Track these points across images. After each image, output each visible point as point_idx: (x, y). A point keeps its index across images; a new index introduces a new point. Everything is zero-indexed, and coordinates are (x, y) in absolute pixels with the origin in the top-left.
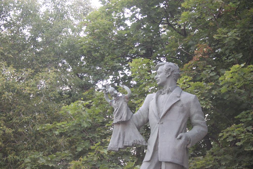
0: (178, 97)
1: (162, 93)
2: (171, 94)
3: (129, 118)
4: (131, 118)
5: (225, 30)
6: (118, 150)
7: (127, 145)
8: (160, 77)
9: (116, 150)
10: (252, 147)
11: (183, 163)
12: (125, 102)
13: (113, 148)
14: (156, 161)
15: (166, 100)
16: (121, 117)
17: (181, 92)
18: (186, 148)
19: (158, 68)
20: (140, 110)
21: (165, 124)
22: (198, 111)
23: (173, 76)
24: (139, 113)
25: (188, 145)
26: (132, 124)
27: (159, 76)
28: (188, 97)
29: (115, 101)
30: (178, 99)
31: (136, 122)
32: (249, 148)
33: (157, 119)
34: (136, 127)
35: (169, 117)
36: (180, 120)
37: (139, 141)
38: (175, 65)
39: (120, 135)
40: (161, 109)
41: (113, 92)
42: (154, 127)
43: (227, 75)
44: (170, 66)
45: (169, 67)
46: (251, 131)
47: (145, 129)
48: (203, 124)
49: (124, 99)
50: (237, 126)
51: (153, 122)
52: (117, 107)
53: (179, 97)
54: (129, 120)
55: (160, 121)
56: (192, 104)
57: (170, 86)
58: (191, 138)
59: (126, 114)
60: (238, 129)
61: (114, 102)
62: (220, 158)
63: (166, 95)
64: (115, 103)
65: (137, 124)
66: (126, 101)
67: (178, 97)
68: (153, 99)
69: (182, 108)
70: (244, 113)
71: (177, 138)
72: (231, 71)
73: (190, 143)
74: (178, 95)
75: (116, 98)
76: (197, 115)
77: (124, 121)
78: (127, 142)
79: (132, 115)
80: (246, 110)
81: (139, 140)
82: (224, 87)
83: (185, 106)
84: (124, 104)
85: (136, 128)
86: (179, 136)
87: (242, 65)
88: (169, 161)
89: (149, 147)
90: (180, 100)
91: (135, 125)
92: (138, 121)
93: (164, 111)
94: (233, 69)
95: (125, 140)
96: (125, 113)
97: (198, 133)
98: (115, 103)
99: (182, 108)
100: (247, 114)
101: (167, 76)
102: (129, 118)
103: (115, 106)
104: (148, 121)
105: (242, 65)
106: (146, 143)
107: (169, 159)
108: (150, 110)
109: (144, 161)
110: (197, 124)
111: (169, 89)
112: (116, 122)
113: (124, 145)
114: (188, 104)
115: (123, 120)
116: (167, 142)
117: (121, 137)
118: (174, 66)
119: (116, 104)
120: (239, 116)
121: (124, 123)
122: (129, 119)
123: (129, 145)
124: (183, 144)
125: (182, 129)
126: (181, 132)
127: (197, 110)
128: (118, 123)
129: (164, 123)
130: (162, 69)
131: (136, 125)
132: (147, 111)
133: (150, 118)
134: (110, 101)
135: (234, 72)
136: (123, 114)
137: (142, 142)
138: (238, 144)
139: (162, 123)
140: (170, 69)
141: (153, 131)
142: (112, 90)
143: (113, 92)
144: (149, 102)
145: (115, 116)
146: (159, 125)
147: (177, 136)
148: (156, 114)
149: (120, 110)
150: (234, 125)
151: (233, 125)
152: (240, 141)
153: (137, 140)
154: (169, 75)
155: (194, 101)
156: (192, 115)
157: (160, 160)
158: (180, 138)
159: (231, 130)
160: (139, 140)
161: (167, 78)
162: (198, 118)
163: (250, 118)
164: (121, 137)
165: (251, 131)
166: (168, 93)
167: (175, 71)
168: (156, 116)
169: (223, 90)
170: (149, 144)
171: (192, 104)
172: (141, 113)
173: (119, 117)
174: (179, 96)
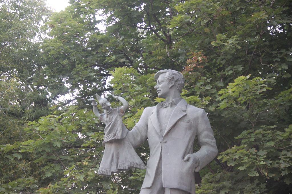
0: (183, 111)
1: (164, 107)
2: (176, 107)
3: (124, 135)
4: (127, 136)
5: (224, 36)
6: (110, 174)
7: (122, 168)
8: (162, 87)
9: (108, 174)
10: (257, 172)
11: (191, 190)
12: (120, 116)
13: (105, 172)
14: (158, 186)
15: (169, 114)
16: (115, 134)
17: (187, 105)
18: (194, 171)
19: (158, 77)
20: (137, 127)
21: (169, 143)
22: (207, 128)
23: (177, 86)
24: (136, 130)
25: (196, 168)
26: (127, 142)
27: (160, 86)
28: (196, 112)
29: (107, 115)
30: (184, 114)
31: (132, 140)
32: (254, 174)
33: (159, 137)
34: (132, 147)
35: (173, 135)
36: (187, 139)
37: (137, 164)
38: (179, 73)
39: (113, 156)
40: (164, 125)
41: (105, 104)
42: (155, 147)
43: (231, 89)
44: (173, 74)
45: (173, 76)
46: (255, 153)
47: (143, 148)
48: (212, 143)
49: (119, 112)
50: (238, 147)
51: (154, 140)
52: (110, 122)
53: (185, 111)
54: (125, 138)
55: (163, 140)
56: (200, 119)
57: (173, 98)
58: (200, 160)
59: (121, 131)
60: (241, 151)
61: (106, 115)
62: (218, 185)
63: (169, 108)
64: (106, 118)
65: (133, 143)
66: (121, 115)
67: (183, 111)
68: (152, 113)
69: (189, 124)
70: (245, 132)
71: (184, 160)
72: (235, 84)
73: (198, 166)
74: (184, 109)
75: (108, 112)
76: (205, 133)
77: (118, 139)
78: (123, 165)
79: (128, 132)
80: (246, 129)
81: (136, 163)
82: (223, 102)
83: (192, 122)
84: (118, 119)
85: (133, 148)
86: (186, 158)
87: (248, 77)
88: (175, 187)
89: (149, 171)
90: (186, 115)
91: (131, 144)
92: (134, 139)
93: (166, 129)
94: (237, 81)
95: (119, 162)
96: (120, 129)
97: (208, 154)
98: (106, 118)
99: (189, 124)
100: (249, 133)
101: (170, 86)
102: (124, 135)
103: (107, 122)
104: (147, 138)
105: (248, 77)
106: (144, 167)
107: (175, 185)
108: (149, 127)
109: (142, 187)
110: (206, 143)
111: (173, 101)
112: (109, 140)
113: (118, 168)
114: (196, 119)
115: (117, 138)
116: (171, 163)
117: (115, 159)
118: (178, 74)
119: (108, 119)
120: (240, 137)
121: (118, 142)
122: (124, 137)
123: (125, 168)
124: (191, 167)
125: (189, 149)
126: (188, 153)
127: (205, 128)
128: (111, 142)
129: (168, 143)
130: (164, 77)
131: (132, 144)
132: (146, 128)
133: (149, 136)
134: (100, 115)
135: (238, 85)
136: (117, 130)
137: (140, 165)
138: (241, 168)
139: (166, 142)
140: (173, 78)
141: (154, 151)
142: (104, 101)
143: (105, 104)
144: (148, 117)
145: (106, 133)
146: (161, 144)
147: (183, 157)
148: (158, 131)
149: (114, 126)
150: (235, 147)
151: (234, 147)
152: (243, 166)
153: (134, 163)
154: (172, 85)
155: (203, 116)
156: (200, 133)
157: (164, 186)
158: (188, 160)
159: (232, 152)
160: (136, 163)
161: (170, 88)
162: (207, 136)
163: (252, 139)
164: (115, 159)
165: (255, 153)
166: (171, 106)
167: (179, 80)
168: (157, 134)
169: (223, 105)
170: (149, 168)
171: (200, 119)
172: (138, 129)
173: (112, 134)
174: (185, 110)
